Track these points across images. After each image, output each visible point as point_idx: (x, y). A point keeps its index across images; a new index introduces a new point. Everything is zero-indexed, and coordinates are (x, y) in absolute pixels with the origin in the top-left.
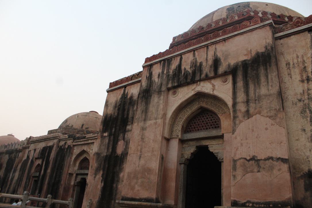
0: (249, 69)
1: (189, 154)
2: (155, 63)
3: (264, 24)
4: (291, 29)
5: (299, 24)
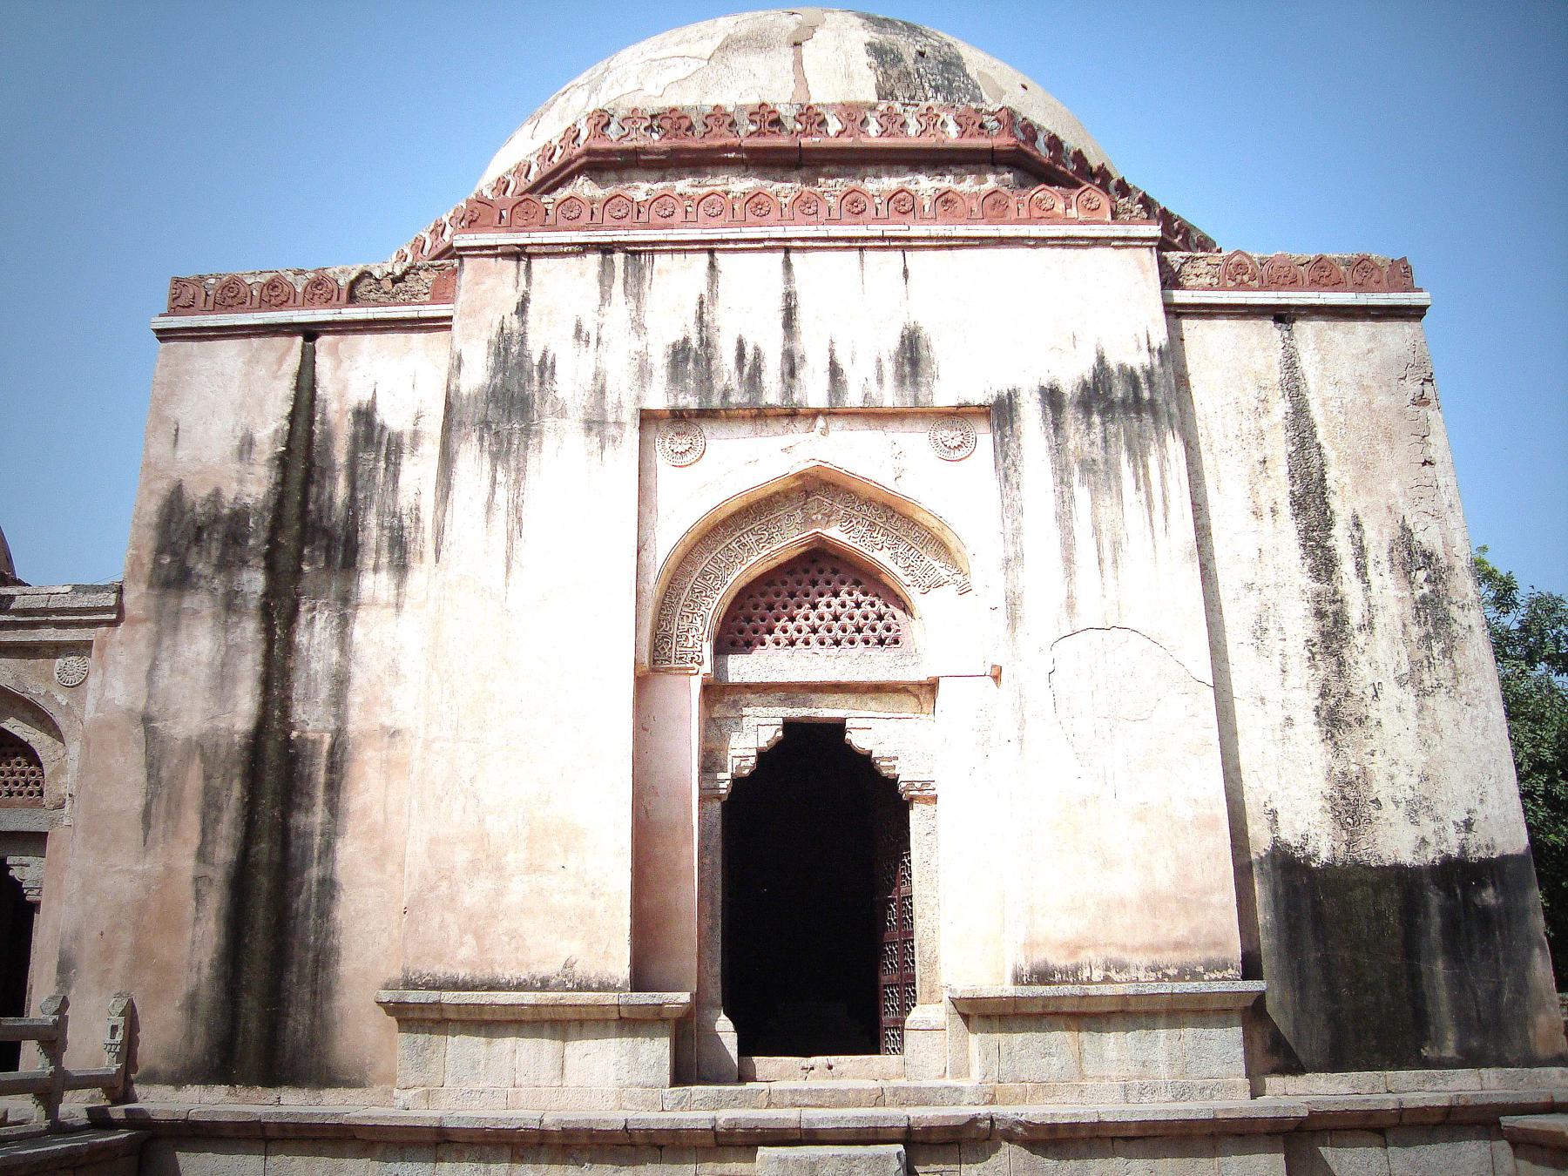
0: (1070, 414)
1: (748, 753)
2: (544, 249)
3: (1131, 235)
4: (1210, 287)
5: (1246, 278)
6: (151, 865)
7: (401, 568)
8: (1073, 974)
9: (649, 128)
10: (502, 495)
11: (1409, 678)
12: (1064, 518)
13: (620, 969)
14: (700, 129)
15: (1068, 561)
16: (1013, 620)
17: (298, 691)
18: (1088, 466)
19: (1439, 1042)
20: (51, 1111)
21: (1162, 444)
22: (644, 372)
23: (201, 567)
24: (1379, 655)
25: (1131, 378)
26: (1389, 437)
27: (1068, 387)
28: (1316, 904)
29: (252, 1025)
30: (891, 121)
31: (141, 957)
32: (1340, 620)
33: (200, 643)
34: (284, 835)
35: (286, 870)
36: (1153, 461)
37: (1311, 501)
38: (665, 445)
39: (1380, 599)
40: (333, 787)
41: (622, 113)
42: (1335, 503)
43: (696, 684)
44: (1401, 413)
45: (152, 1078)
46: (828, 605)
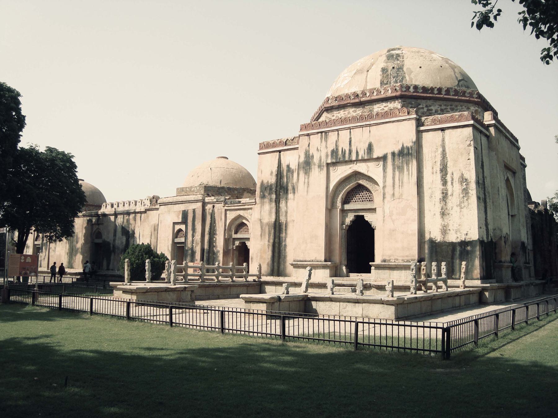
0: (396, 157)
4: (431, 125)
6: (262, 243)
7: (294, 193)
8: (389, 261)
9: (336, 100)
10: (306, 180)
11: (460, 205)
12: (394, 178)
13: (323, 259)
14: (344, 99)
15: (394, 186)
16: (384, 198)
17: (280, 214)
18: (399, 167)
19: (456, 275)
20: (246, 279)
21: (412, 162)
22: (327, 156)
23: (266, 194)
24: (453, 201)
25: (408, 148)
26: (462, 154)
27: (396, 152)
28: (436, 249)
29: (276, 267)
30: (379, 92)
31: (261, 257)
32: (447, 194)
33: (267, 207)
34: (279, 238)
35: (280, 243)
36: (410, 166)
37: (444, 170)
38: (331, 169)
39: (455, 189)
40: (286, 230)
41: (331, 97)
42: (448, 170)
43: (338, 210)
44: (465, 149)
45: (263, 275)
46: (362, 194)
